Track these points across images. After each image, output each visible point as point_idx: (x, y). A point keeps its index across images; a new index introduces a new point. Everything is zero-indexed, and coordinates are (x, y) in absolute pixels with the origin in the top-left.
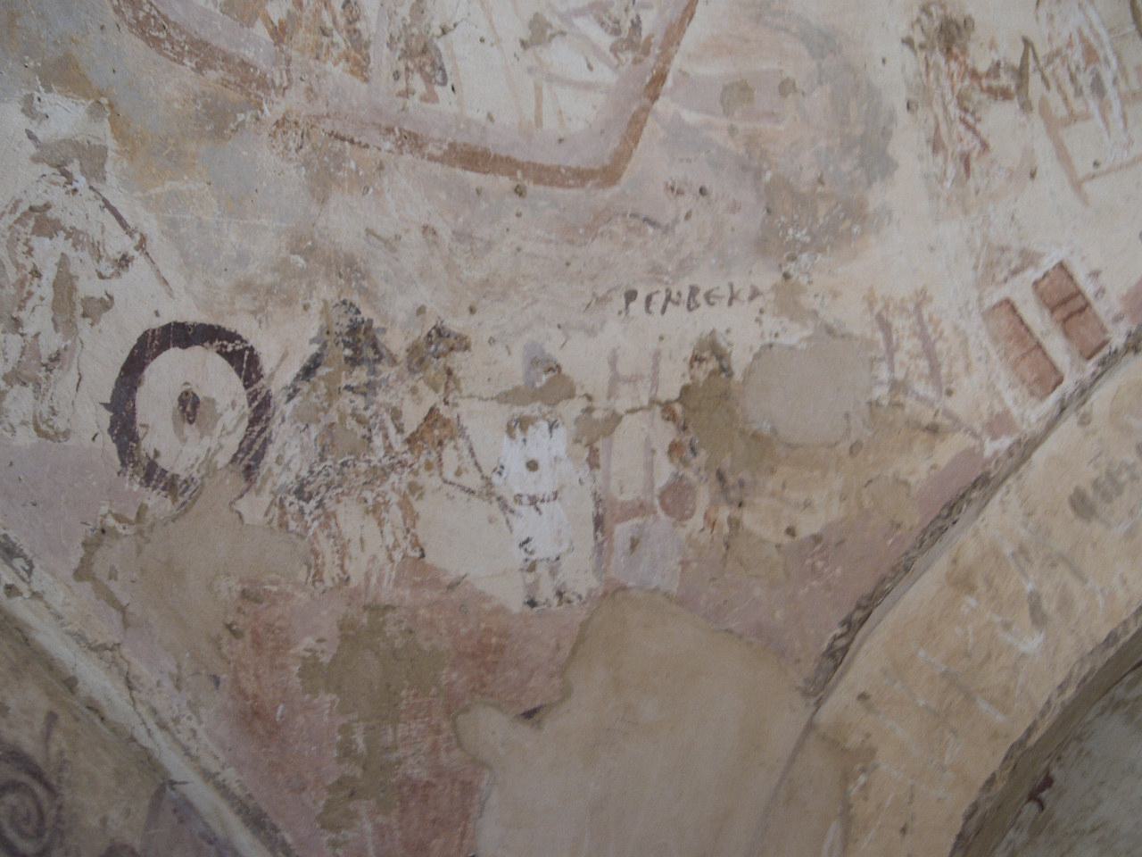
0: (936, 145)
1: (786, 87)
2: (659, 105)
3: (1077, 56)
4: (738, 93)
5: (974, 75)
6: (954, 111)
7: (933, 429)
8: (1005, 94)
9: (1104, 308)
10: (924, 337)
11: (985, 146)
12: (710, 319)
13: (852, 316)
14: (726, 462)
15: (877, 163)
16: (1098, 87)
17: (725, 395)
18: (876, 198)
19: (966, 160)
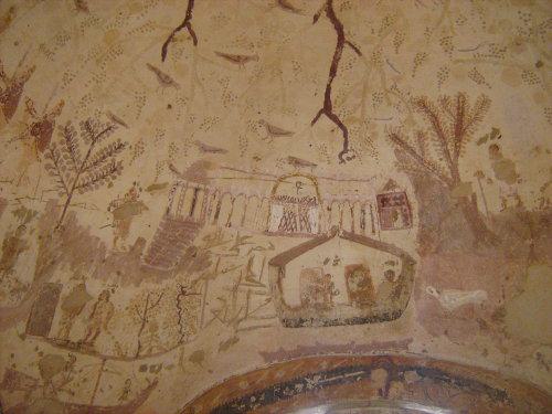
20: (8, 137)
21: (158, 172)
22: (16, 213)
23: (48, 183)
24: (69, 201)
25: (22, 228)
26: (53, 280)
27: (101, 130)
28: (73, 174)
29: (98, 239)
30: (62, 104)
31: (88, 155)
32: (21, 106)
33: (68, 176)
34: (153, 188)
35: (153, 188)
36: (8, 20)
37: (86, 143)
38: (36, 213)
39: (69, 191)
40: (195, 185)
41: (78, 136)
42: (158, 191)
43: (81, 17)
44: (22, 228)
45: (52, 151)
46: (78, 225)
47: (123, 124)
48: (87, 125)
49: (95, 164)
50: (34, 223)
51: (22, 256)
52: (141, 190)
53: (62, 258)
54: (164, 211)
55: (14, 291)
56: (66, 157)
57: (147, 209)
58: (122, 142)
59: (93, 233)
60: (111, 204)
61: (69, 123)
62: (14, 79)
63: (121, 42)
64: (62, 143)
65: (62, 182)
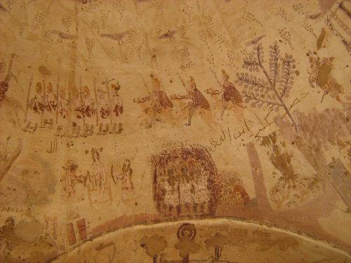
0: (65, 189)
1: (36, 172)
2: (8, 172)
3: (98, 177)
4: (25, 172)
5: (76, 177)
6: (70, 182)
7: (51, 245)
8: (81, 182)
9: (88, 230)
10: (54, 226)
11: (75, 192)
12: (11, 214)
13: (41, 219)
14: (10, 242)
15: (52, 191)
16: (100, 185)
17: (12, 229)
18: (50, 197)
19: (70, 193)
20: (219, 115)
21: (311, 30)
22: (263, 143)
23: (262, 113)
24: (286, 108)
25: (276, 148)
26: (329, 161)
27: (256, 56)
28: (271, 93)
29: (327, 110)
30: (224, 72)
31: (267, 75)
32: (208, 97)
33: (269, 97)
34: (320, 43)
35: (320, 43)
36: (156, 80)
37: (258, 71)
38: (274, 134)
39: (279, 103)
40: (336, 6)
41: (250, 73)
42: (325, 40)
43: (177, 36)
44: (276, 148)
45: (246, 96)
46: (307, 115)
47: (261, 38)
48: (247, 63)
49: (276, 73)
50: (279, 140)
51: (293, 163)
52: (315, 53)
53: (319, 143)
54: (342, 45)
55: (311, 186)
56: (257, 90)
57: (332, 59)
58: (273, 45)
59: (321, 109)
60: (310, 82)
61: (237, 74)
62: (190, 93)
63: (203, 15)
64: (246, 87)
65: (270, 103)
